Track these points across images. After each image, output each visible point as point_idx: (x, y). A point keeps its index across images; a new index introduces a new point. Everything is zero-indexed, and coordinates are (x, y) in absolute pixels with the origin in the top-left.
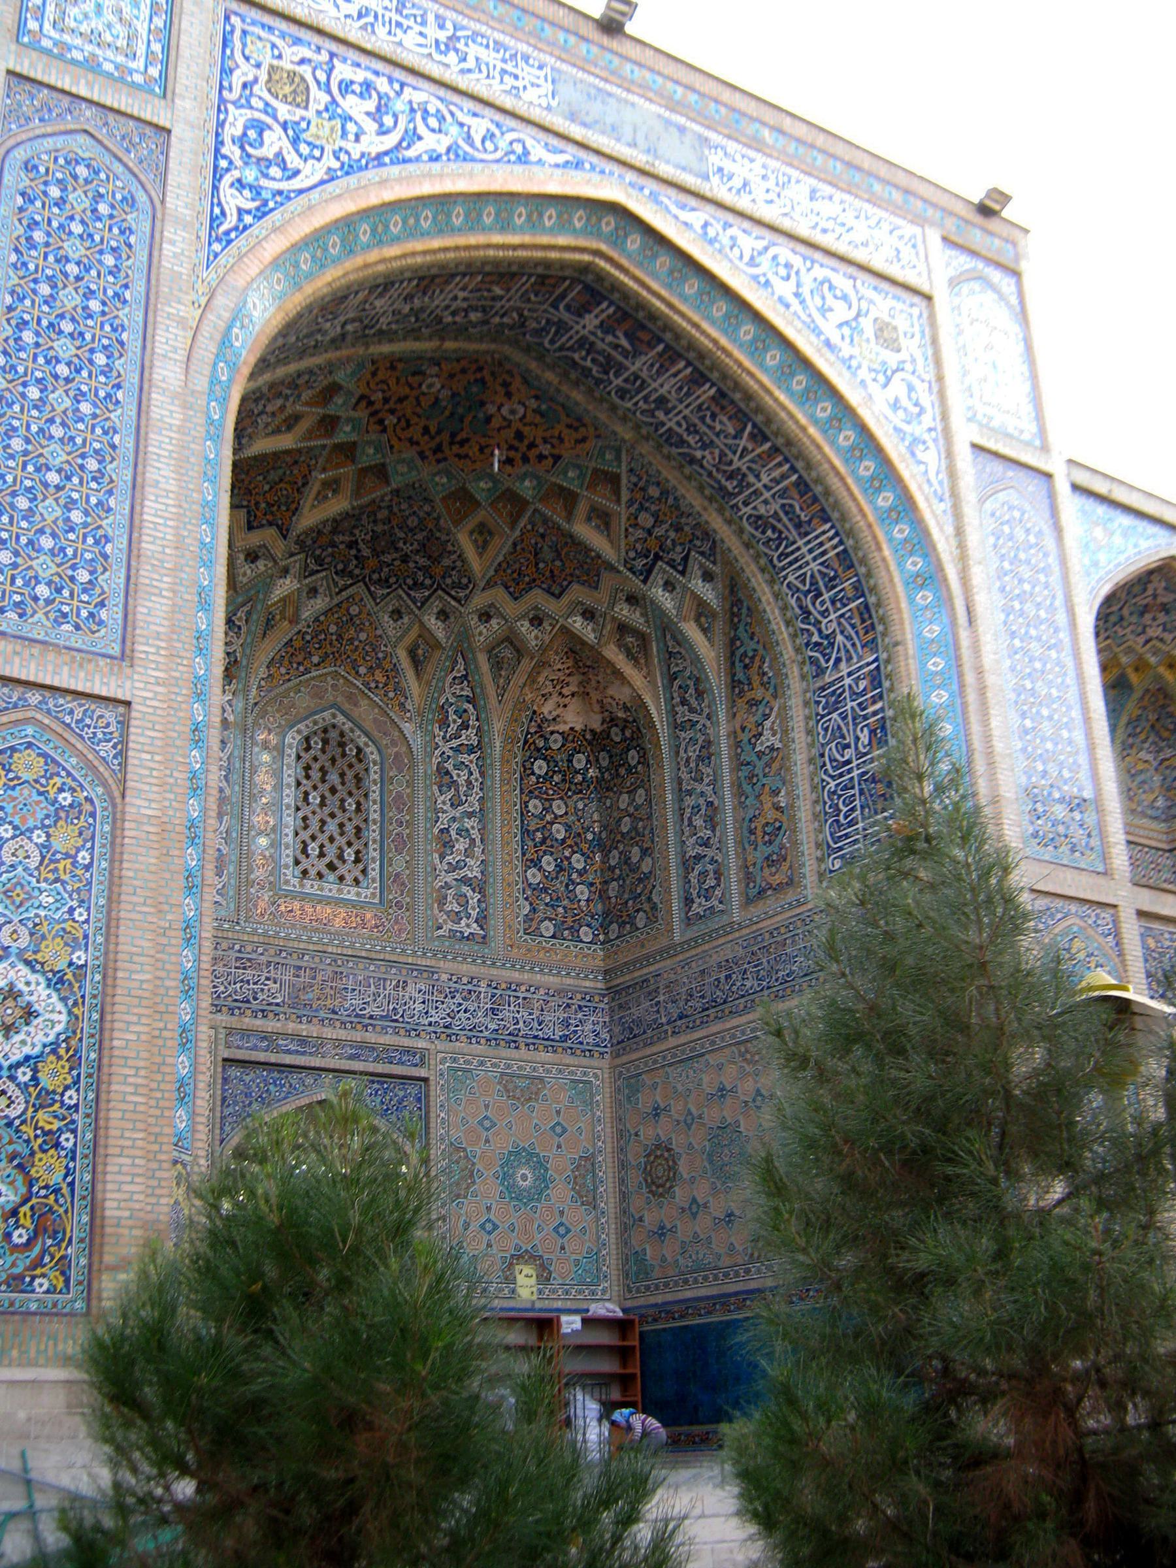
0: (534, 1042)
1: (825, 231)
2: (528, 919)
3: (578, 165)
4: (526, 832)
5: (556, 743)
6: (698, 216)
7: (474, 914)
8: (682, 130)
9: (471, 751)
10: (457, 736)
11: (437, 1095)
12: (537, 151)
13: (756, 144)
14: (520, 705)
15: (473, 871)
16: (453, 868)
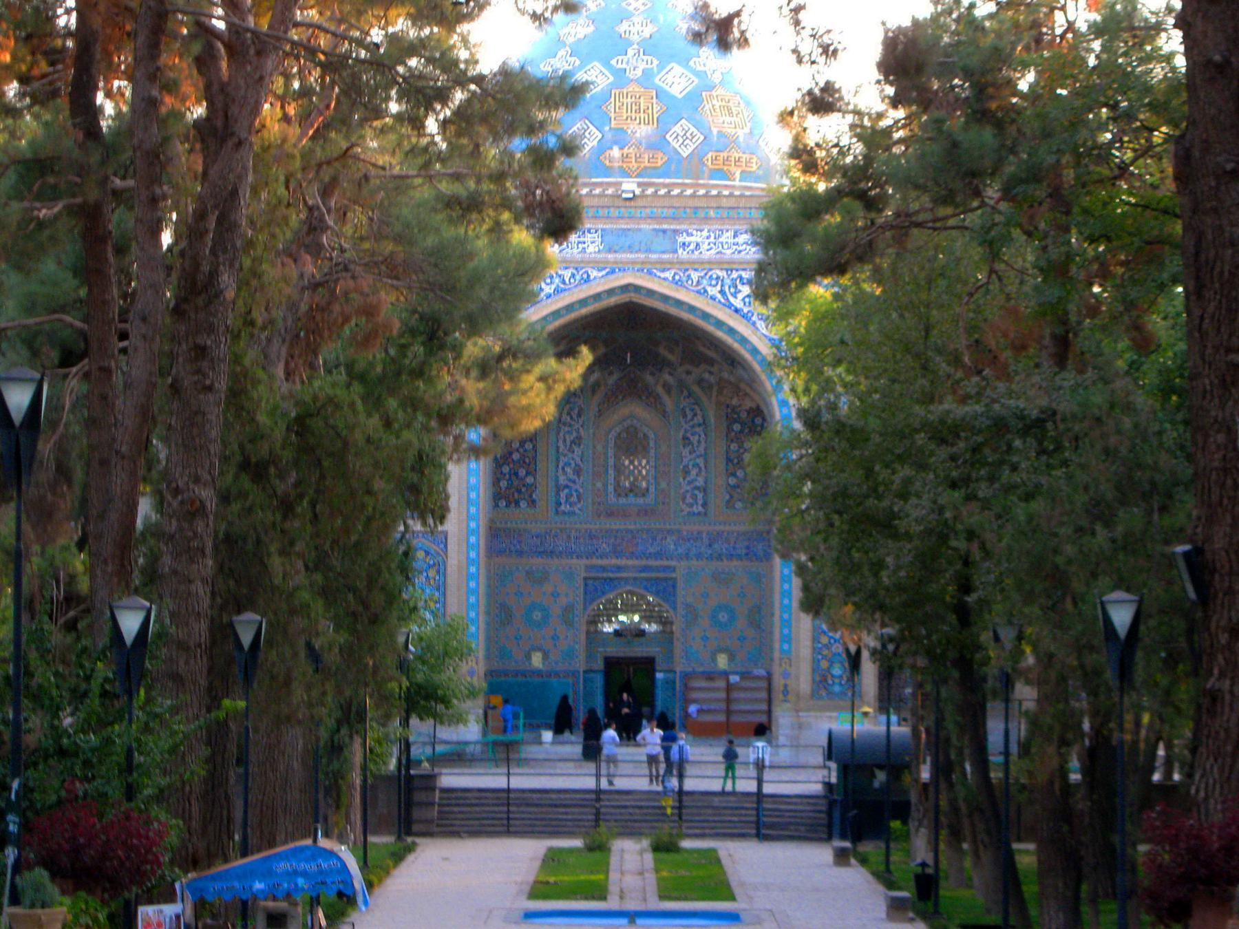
0: (731, 557)
1: (740, 252)
2: (728, 502)
3: (613, 272)
4: (729, 460)
5: (744, 415)
6: (669, 275)
7: (700, 502)
8: (664, 231)
9: (700, 425)
10: (692, 419)
11: (680, 584)
12: (594, 274)
13: (707, 219)
14: (718, 403)
15: (700, 482)
16: (690, 483)
